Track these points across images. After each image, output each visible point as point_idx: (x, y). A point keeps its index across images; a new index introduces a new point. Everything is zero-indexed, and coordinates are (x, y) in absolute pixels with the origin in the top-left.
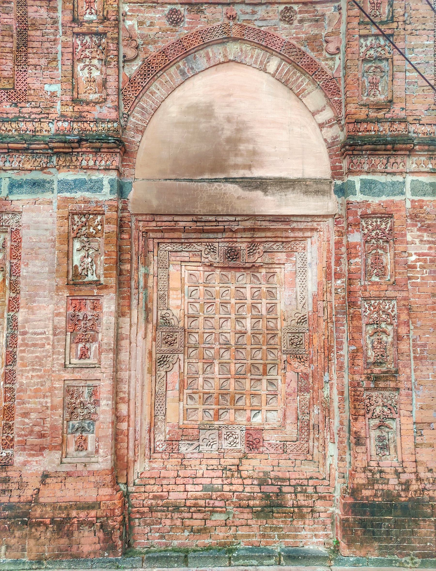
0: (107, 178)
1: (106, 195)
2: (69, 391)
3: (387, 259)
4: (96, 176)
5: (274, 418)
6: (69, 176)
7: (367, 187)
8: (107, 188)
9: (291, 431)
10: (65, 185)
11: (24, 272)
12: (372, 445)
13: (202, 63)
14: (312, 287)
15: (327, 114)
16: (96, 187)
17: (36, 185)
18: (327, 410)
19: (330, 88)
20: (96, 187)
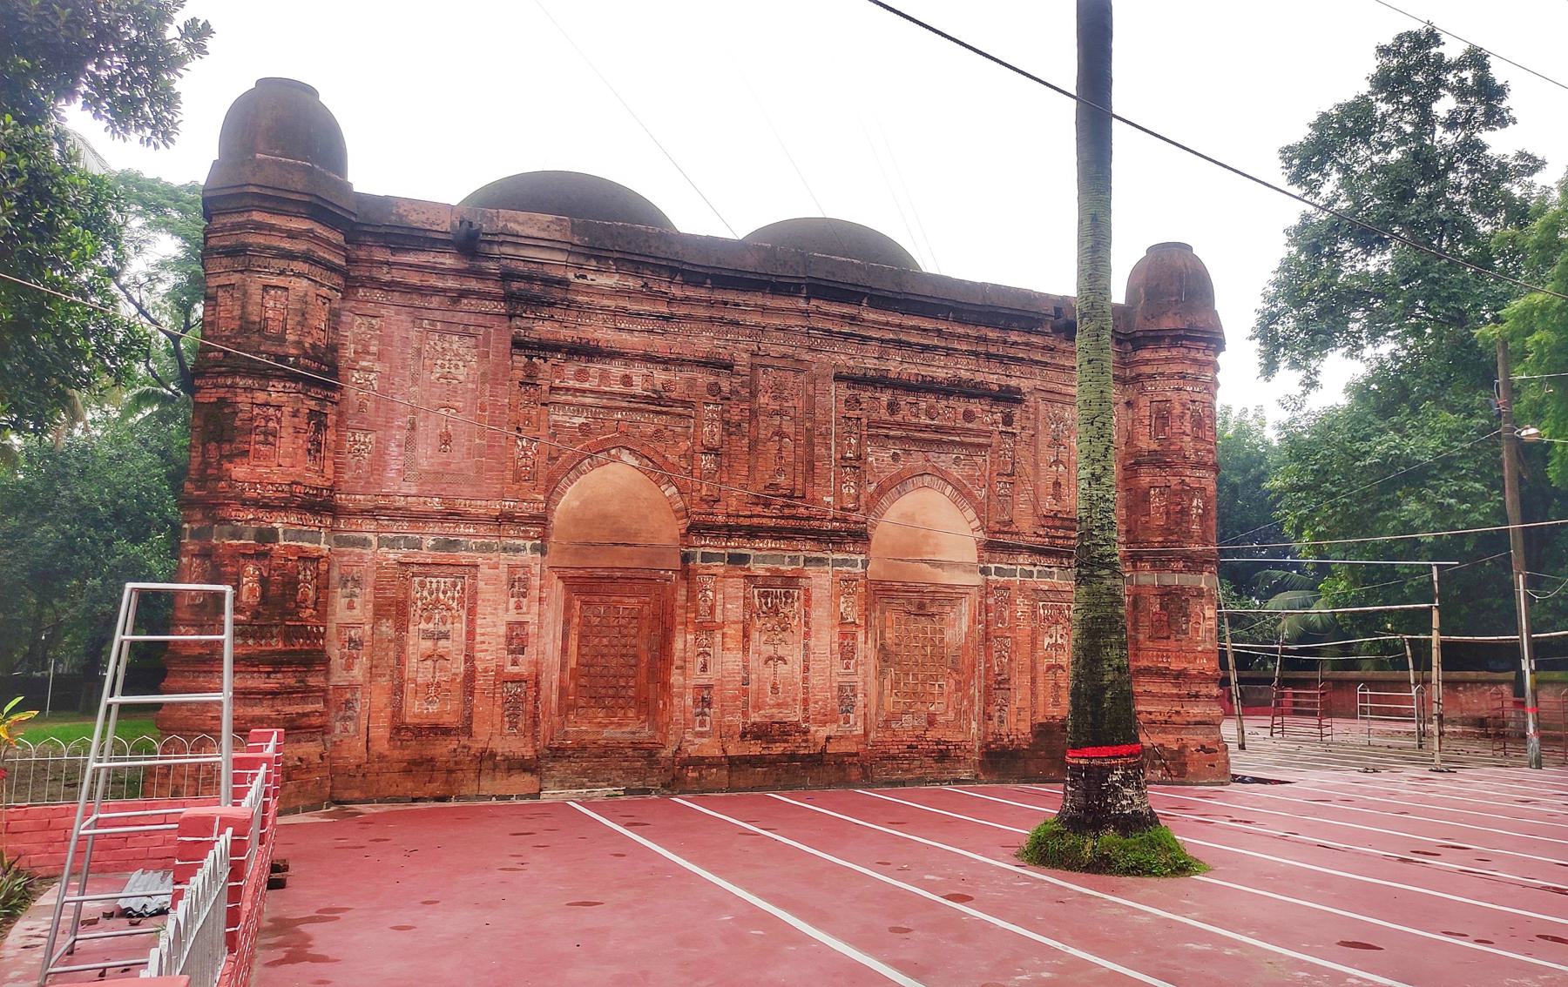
1: (859, 570)
2: (841, 688)
3: (1006, 614)
4: (854, 557)
5: (942, 708)
6: (839, 556)
7: (998, 571)
9: (951, 715)
10: (836, 562)
11: (813, 615)
12: (996, 720)
13: (910, 486)
14: (965, 629)
15: (977, 523)
16: (854, 564)
17: (820, 561)
18: (972, 702)
19: (979, 511)
20: (854, 564)
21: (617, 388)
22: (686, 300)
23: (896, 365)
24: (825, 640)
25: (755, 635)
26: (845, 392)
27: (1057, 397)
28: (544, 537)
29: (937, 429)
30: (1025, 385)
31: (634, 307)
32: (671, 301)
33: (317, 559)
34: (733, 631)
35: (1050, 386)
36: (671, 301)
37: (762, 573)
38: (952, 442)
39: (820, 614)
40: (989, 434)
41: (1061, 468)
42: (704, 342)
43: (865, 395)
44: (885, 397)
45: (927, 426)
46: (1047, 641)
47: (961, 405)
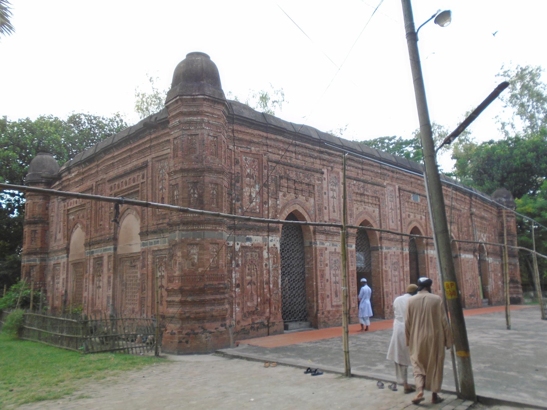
0: (112, 247)
1: (112, 251)
8: (112, 250)
13: (125, 215)
16: (110, 249)
21: (75, 205)
22: (85, 172)
23: (121, 170)
24: (105, 280)
25: (95, 278)
26: (108, 186)
27: (161, 158)
28: (68, 253)
29: (129, 189)
30: (149, 158)
31: (77, 180)
32: (83, 173)
33: (36, 266)
34: (91, 278)
35: (157, 154)
36: (83, 173)
37: (96, 257)
38: (132, 193)
39: (105, 269)
40: (137, 186)
41: (164, 190)
42: (89, 183)
43: (113, 184)
44: (117, 183)
45: (125, 189)
46: (159, 274)
47: (132, 176)
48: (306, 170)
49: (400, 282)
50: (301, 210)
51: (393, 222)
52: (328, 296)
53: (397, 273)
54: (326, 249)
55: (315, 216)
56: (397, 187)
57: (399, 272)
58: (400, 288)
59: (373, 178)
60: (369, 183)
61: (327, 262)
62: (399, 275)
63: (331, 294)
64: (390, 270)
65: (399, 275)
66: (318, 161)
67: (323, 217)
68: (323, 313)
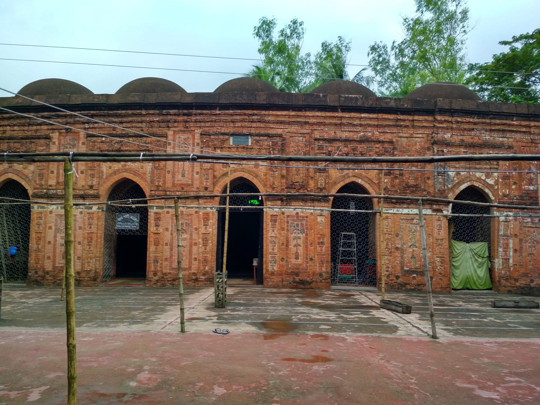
48: (22, 139)
49: (191, 246)
50: (15, 178)
51: (183, 176)
52: (49, 258)
53: (185, 236)
54: (51, 212)
55: (35, 181)
56: (198, 131)
57: (191, 235)
58: (190, 253)
59: (145, 130)
60: (130, 136)
61: (52, 225)
62: (191, 239)
63: (54, 256)
64: (168, 234)
65: (191, 239)
66: (45, 127)
67: (47, 181)
68: (36, 273)
